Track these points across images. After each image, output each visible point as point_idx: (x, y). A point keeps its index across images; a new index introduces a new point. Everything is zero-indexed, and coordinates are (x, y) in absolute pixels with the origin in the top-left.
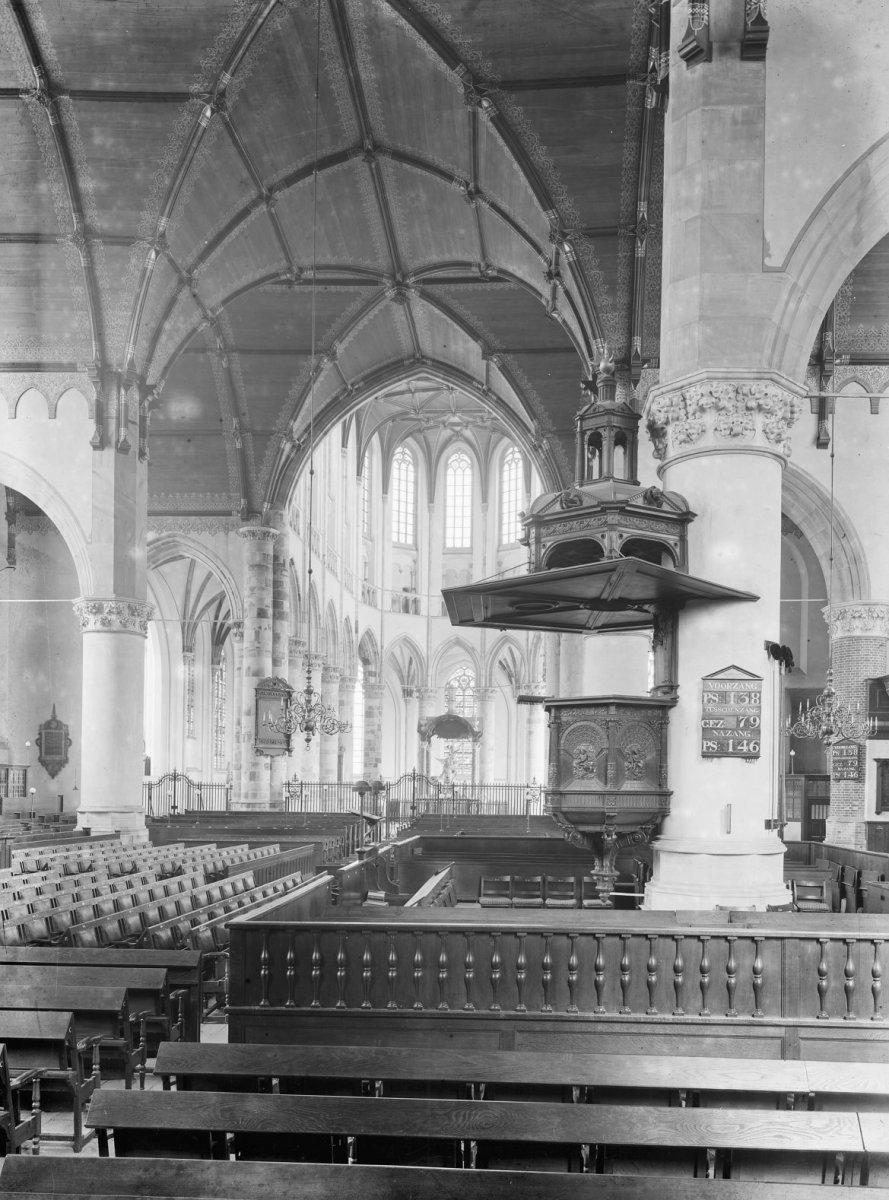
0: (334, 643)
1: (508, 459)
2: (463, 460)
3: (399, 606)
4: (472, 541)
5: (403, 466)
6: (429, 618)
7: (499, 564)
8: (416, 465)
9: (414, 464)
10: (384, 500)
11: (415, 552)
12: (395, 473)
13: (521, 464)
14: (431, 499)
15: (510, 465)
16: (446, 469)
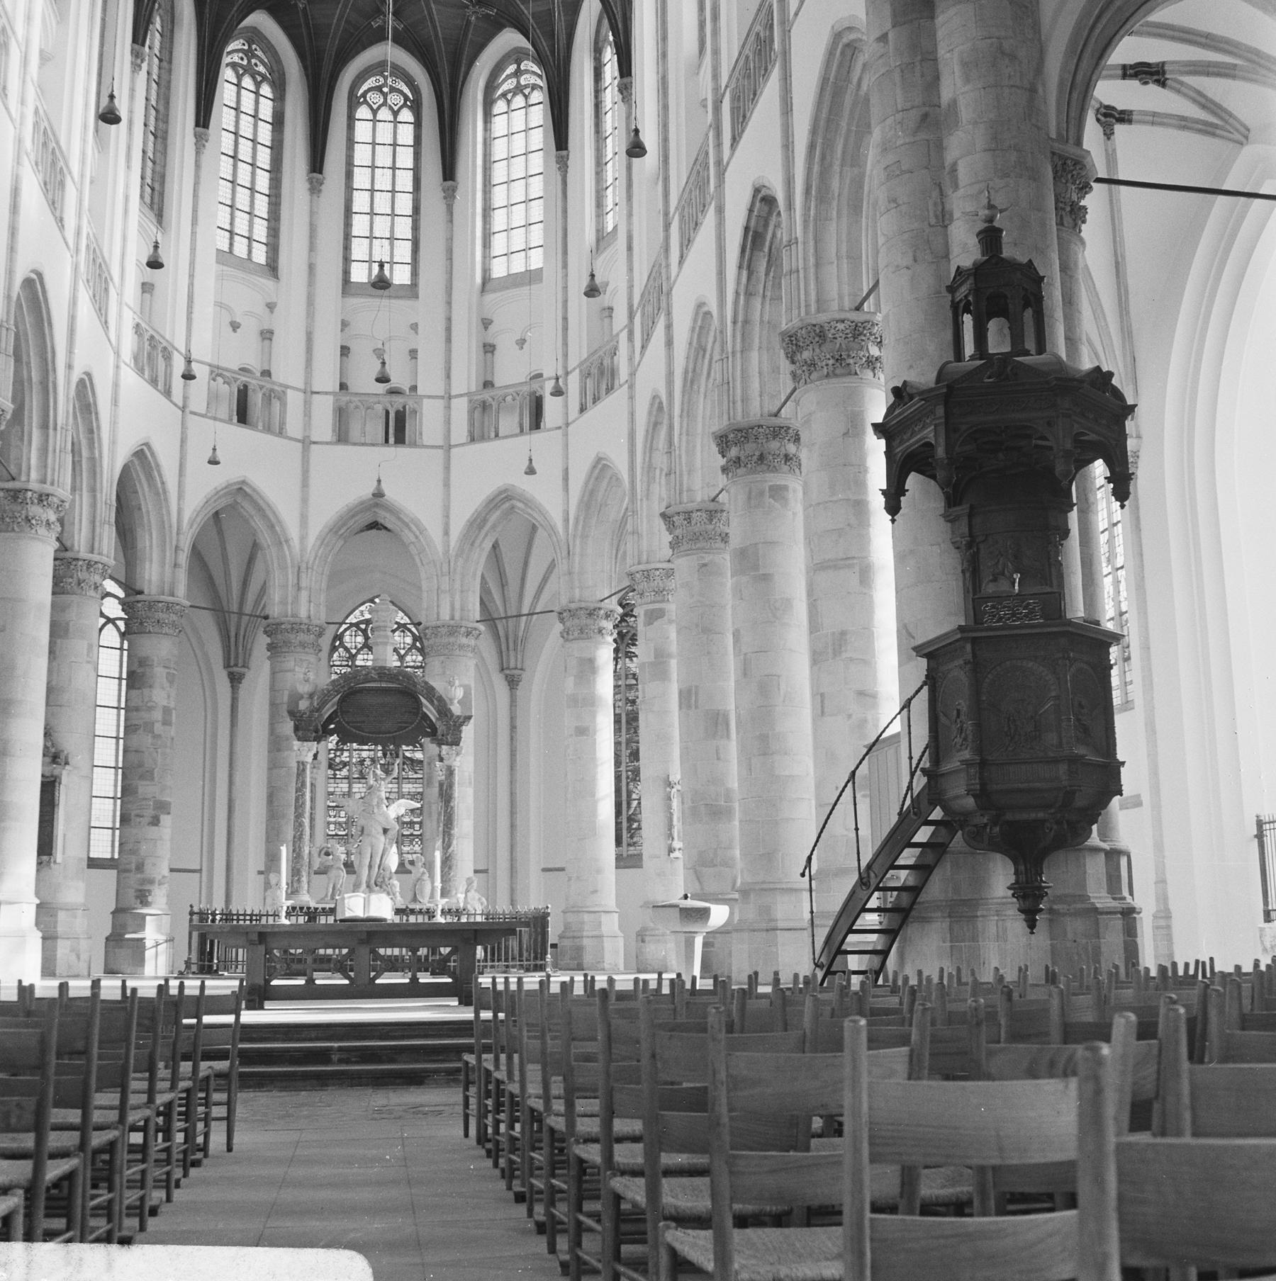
0: (44, 426)
1: (505, 87)
2: (393, 90)
3: (227, 407)
4: (415, 273)
5: (247, 82)
6: (307, 443)
7: (486, 323)
8: (280, 88)
9: (273, 85)
10: (200, 141)
11: (268, 283)
12: (226, 93)
13: (537, 96)
14: (317, 163)
15: (509, 102)
16: (354, 102)
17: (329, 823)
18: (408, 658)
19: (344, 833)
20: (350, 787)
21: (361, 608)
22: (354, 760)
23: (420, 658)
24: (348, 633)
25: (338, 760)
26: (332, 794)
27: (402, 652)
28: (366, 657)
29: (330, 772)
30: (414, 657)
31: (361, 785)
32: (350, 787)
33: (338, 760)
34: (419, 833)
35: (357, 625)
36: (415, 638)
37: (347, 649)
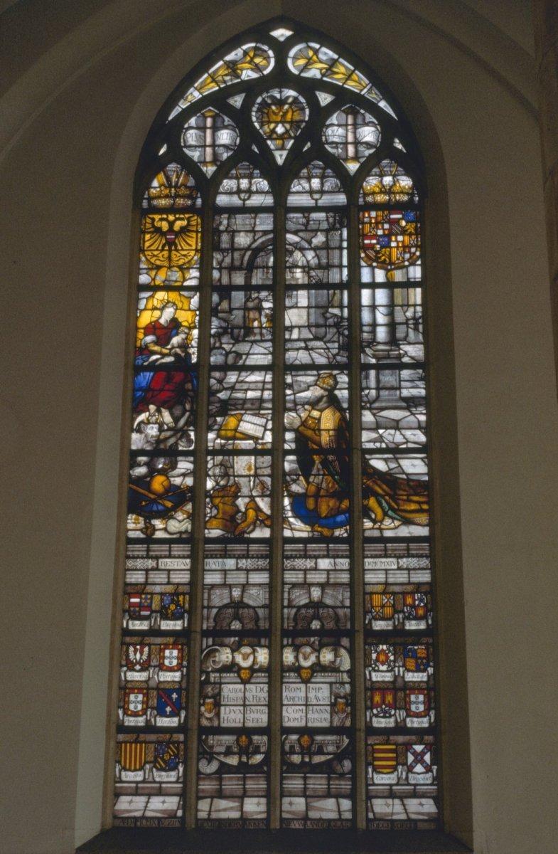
17: (126, 689)
18: (371, 183)
19: (172, 722)
20: (196, 571)
21: (229, 57)
22: (210, 484)
23: (405, 182)
24: (193, 121)
25: (158, 483)
26: (140, 589)
27: (353, 167)
28: (244, 183)
29: (134, 525)
30: (388, 180)
31: (230, 563)
32: (196, 571)
33: (158, 483)
34: (424, 723)
35: (218, 101)
36: (387, 127)
37: (190, 167)
